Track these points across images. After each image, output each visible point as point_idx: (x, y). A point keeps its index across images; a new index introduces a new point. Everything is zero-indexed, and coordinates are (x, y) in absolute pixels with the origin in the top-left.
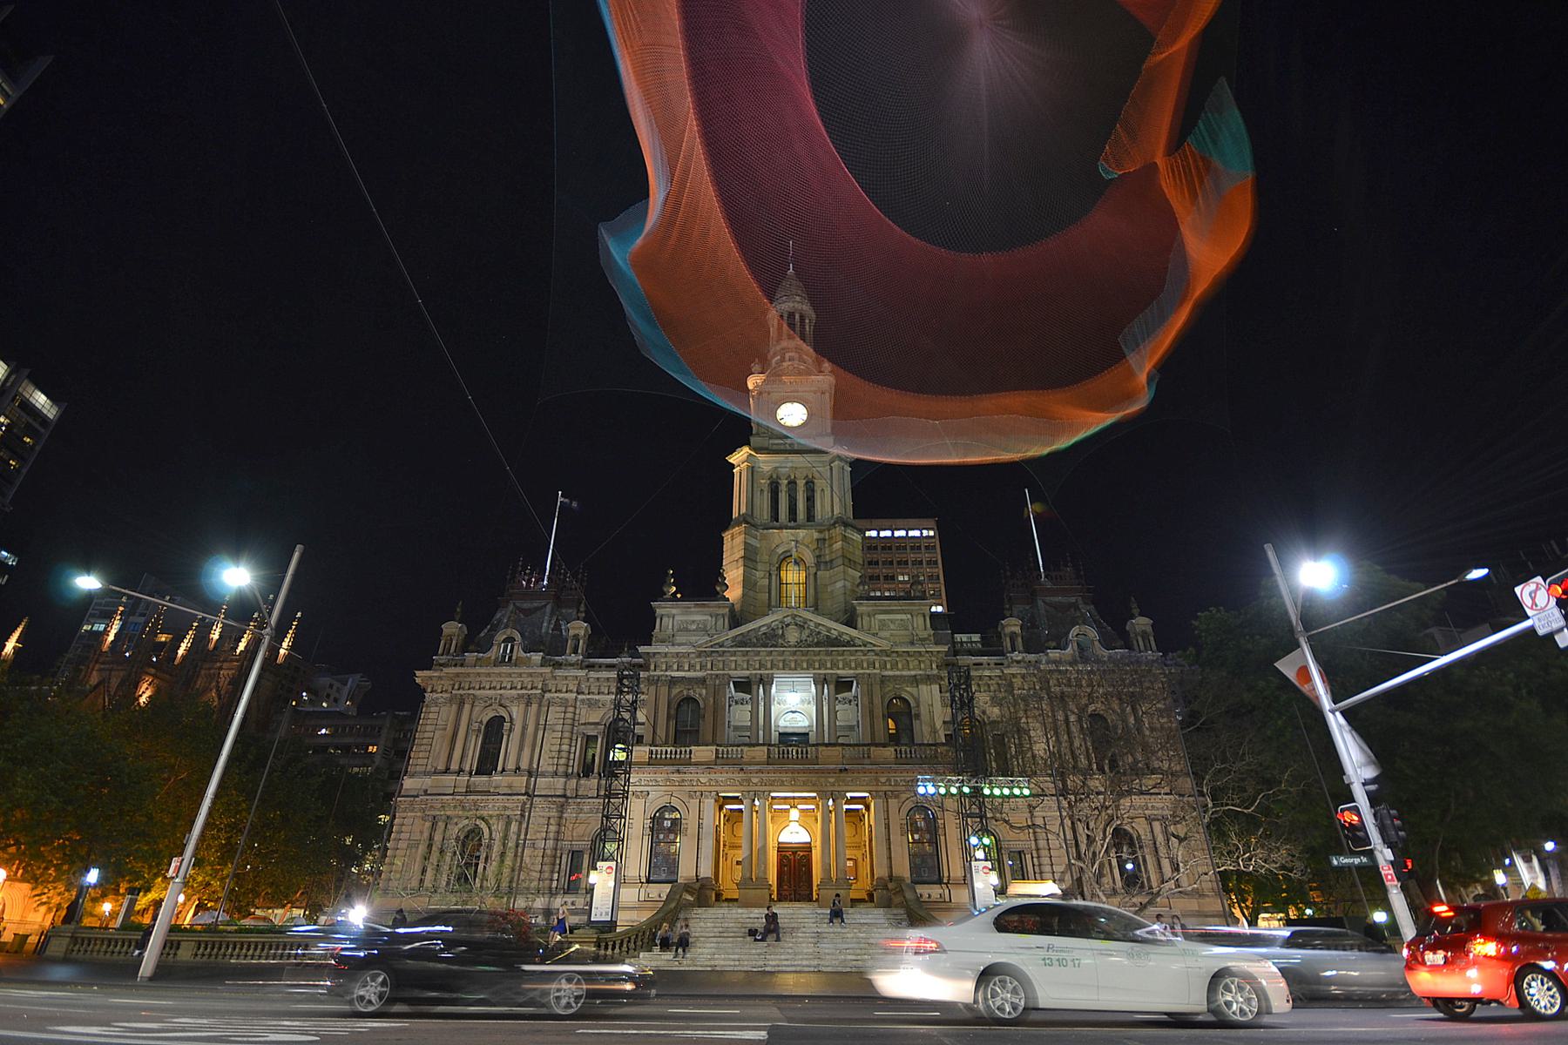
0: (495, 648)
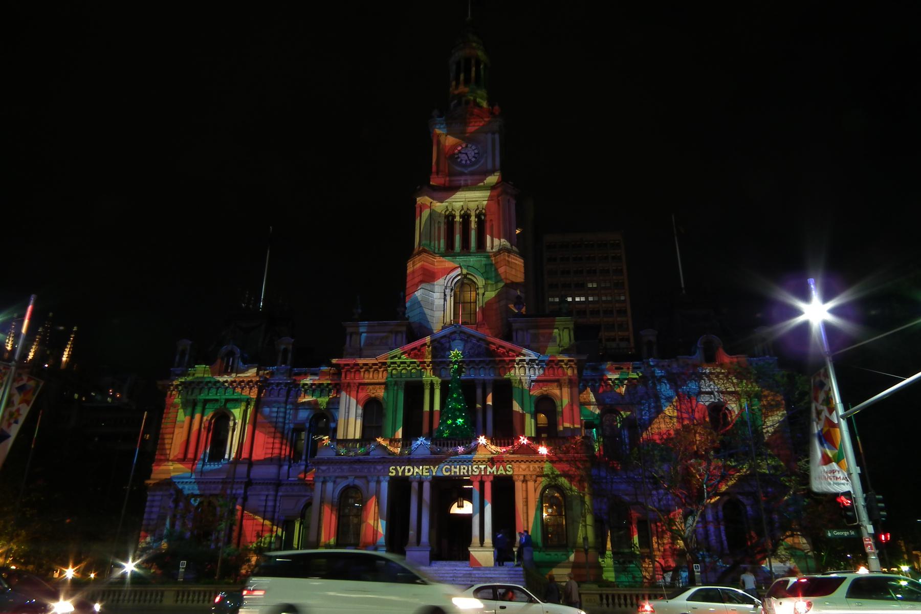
0: (219, 361)
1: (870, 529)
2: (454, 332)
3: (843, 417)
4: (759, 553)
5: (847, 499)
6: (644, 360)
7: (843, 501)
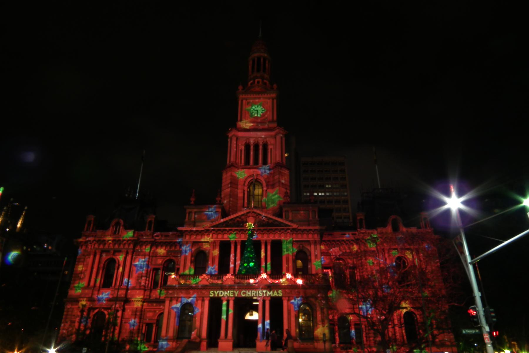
0: (111, 228)
1: (487, 329)
2: (249, 212)
3: (470, 263)
4: (424, 343)
5: (474, 311)
6: (358, 230)
7: (471, 312)
